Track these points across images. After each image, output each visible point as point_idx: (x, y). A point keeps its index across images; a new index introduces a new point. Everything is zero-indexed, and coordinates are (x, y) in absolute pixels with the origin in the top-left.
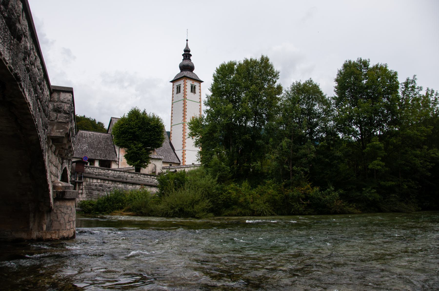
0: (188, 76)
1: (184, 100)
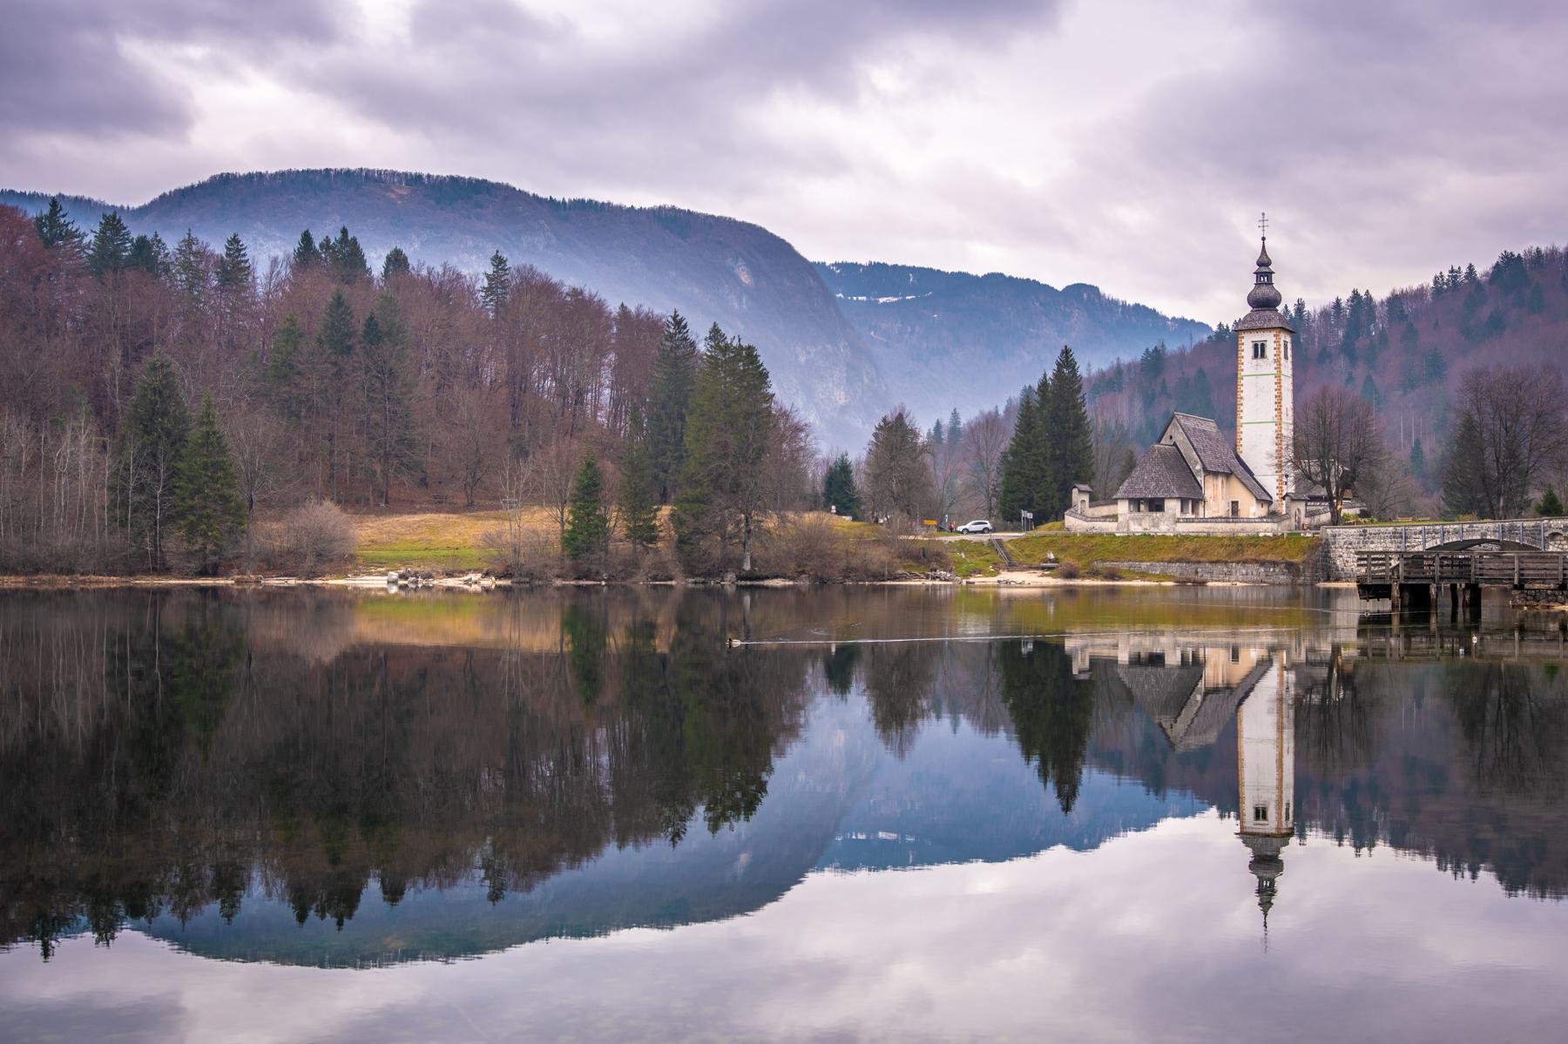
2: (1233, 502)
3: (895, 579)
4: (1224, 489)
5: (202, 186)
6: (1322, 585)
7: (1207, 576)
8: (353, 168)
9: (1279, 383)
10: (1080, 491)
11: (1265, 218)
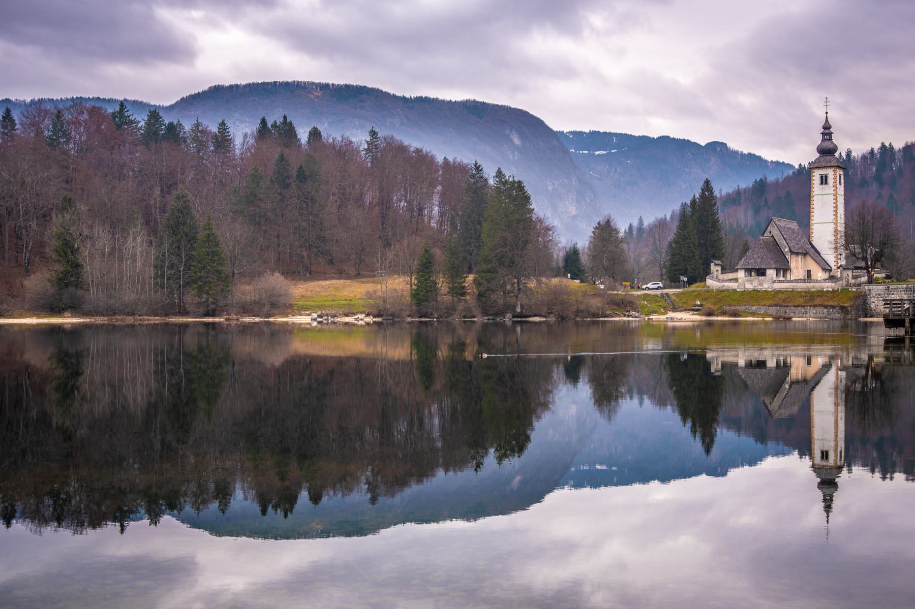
2: (808, 271)
3: (605, 317)
4: (803, 263)
5: (204, 93)
6: (862, 319)
7: (792, 314)
8: (289, 80)
9: (836, 199)
10: (715, 264)
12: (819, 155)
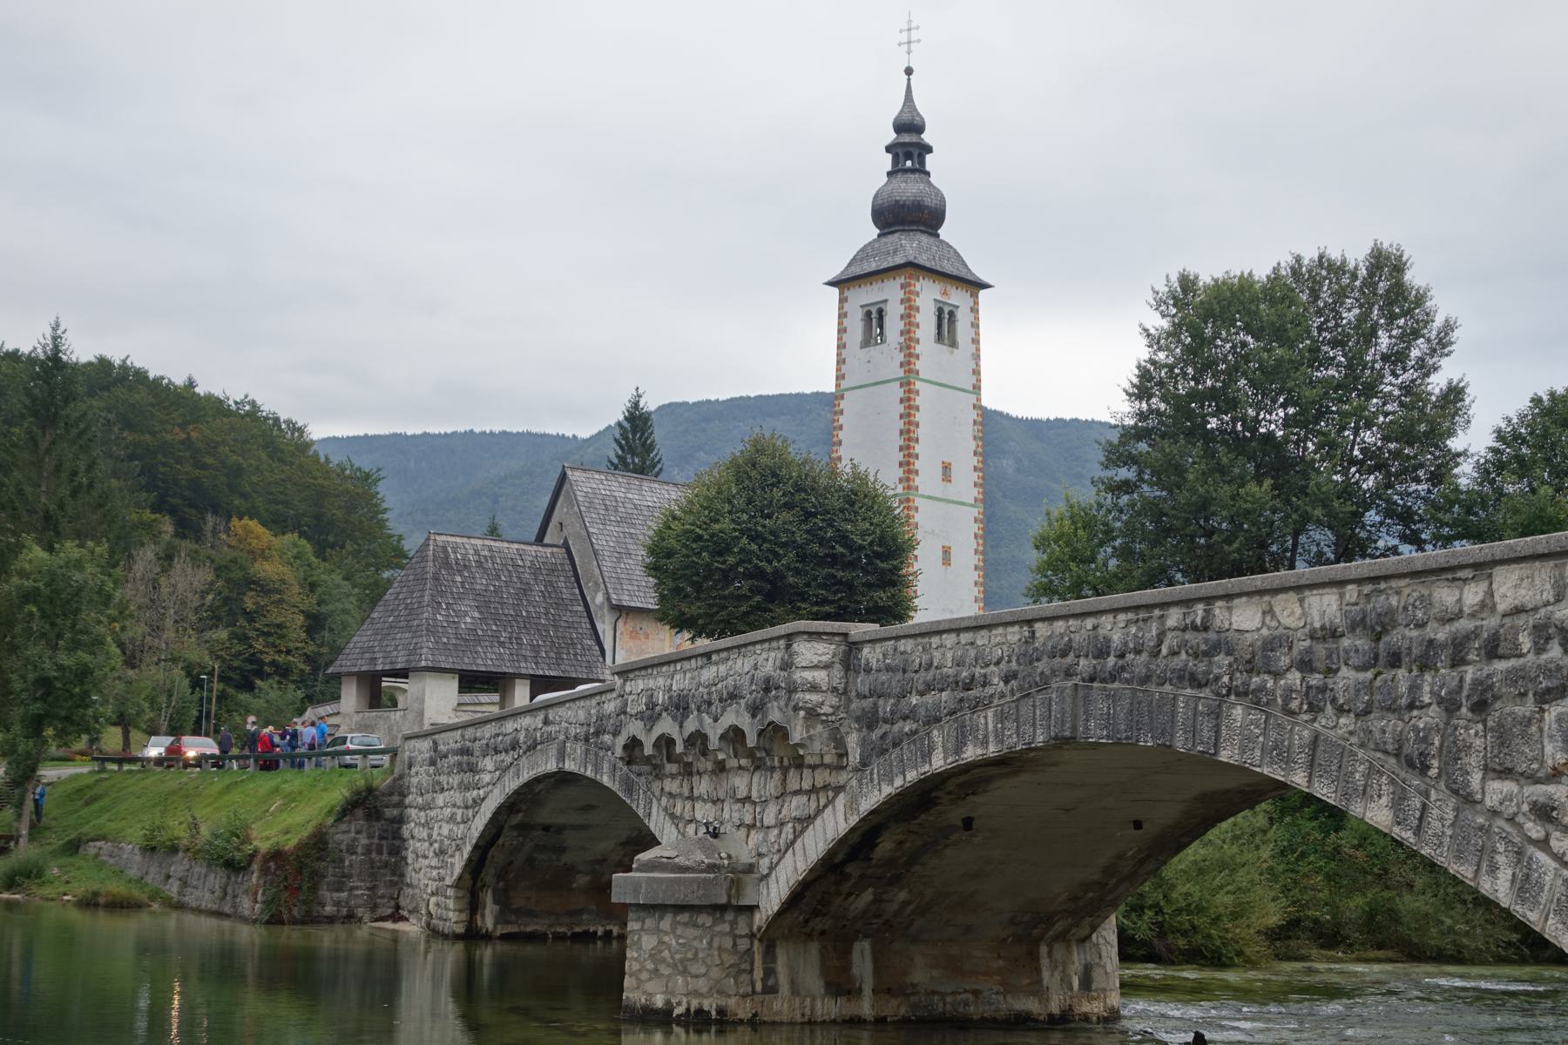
0: (923, 260)
1: (906, 384)
11: (913, 25)
12: (878, 231)
